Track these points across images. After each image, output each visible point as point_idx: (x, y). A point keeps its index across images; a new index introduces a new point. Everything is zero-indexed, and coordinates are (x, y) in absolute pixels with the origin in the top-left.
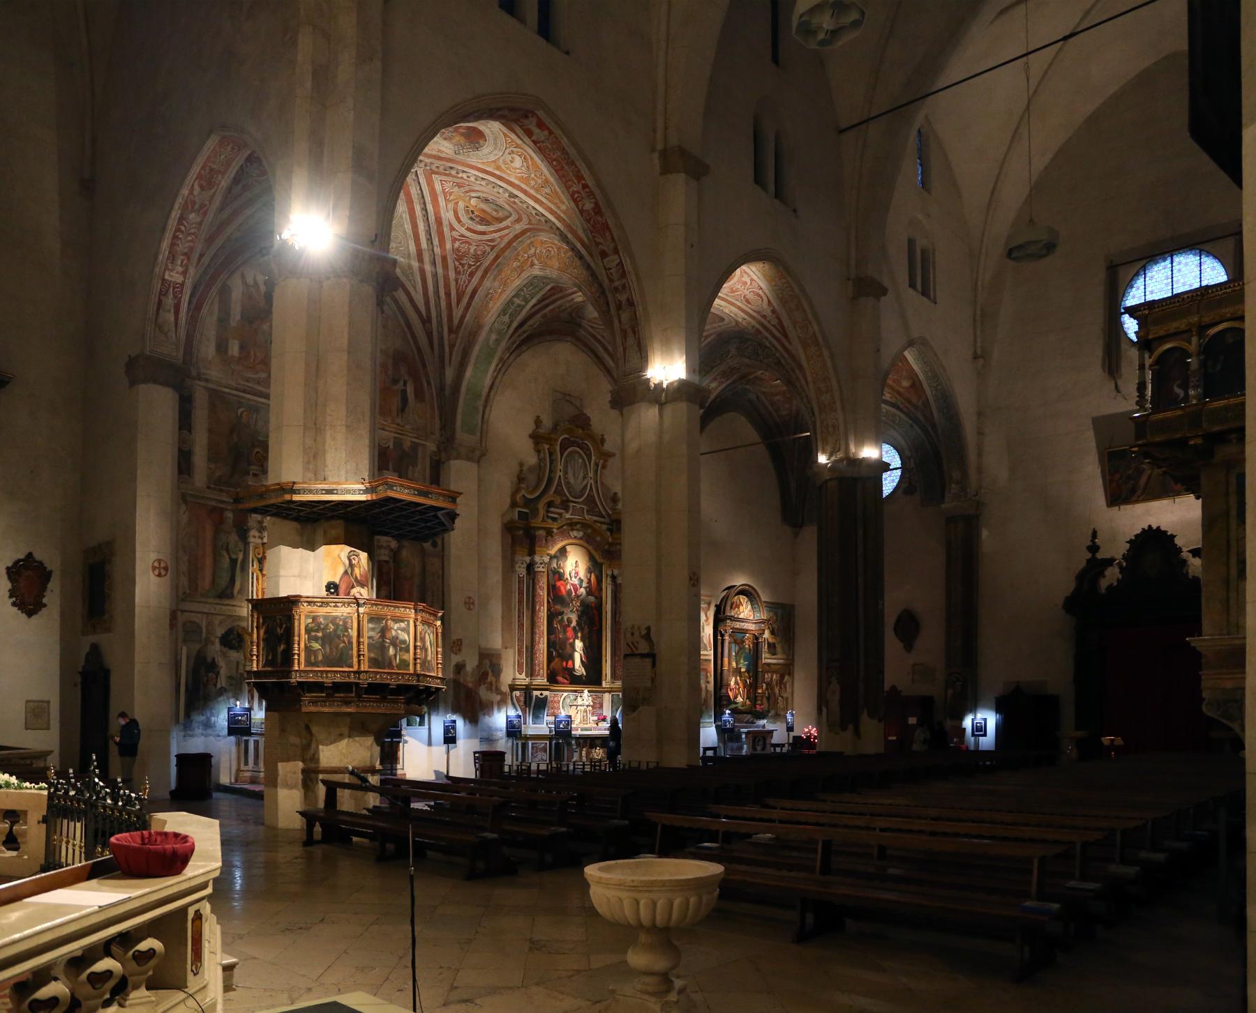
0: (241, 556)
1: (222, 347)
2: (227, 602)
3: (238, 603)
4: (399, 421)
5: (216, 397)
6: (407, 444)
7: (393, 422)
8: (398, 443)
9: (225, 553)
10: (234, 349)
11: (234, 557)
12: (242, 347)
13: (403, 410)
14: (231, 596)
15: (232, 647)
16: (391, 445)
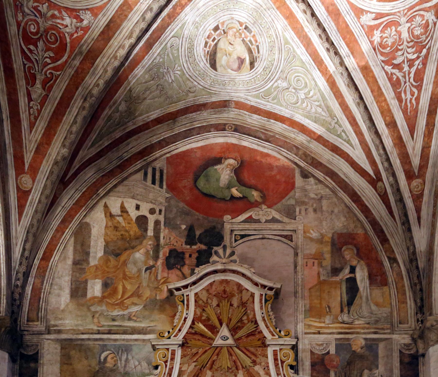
1: (78, 291)
4: (345, 318)
5: (70, 348)
6: (358, 343)
7: (335, 320)
8: (342, 346)
10: (95, 288)
12: (105, 285)
13: (350, 303)
16: (333, 351)
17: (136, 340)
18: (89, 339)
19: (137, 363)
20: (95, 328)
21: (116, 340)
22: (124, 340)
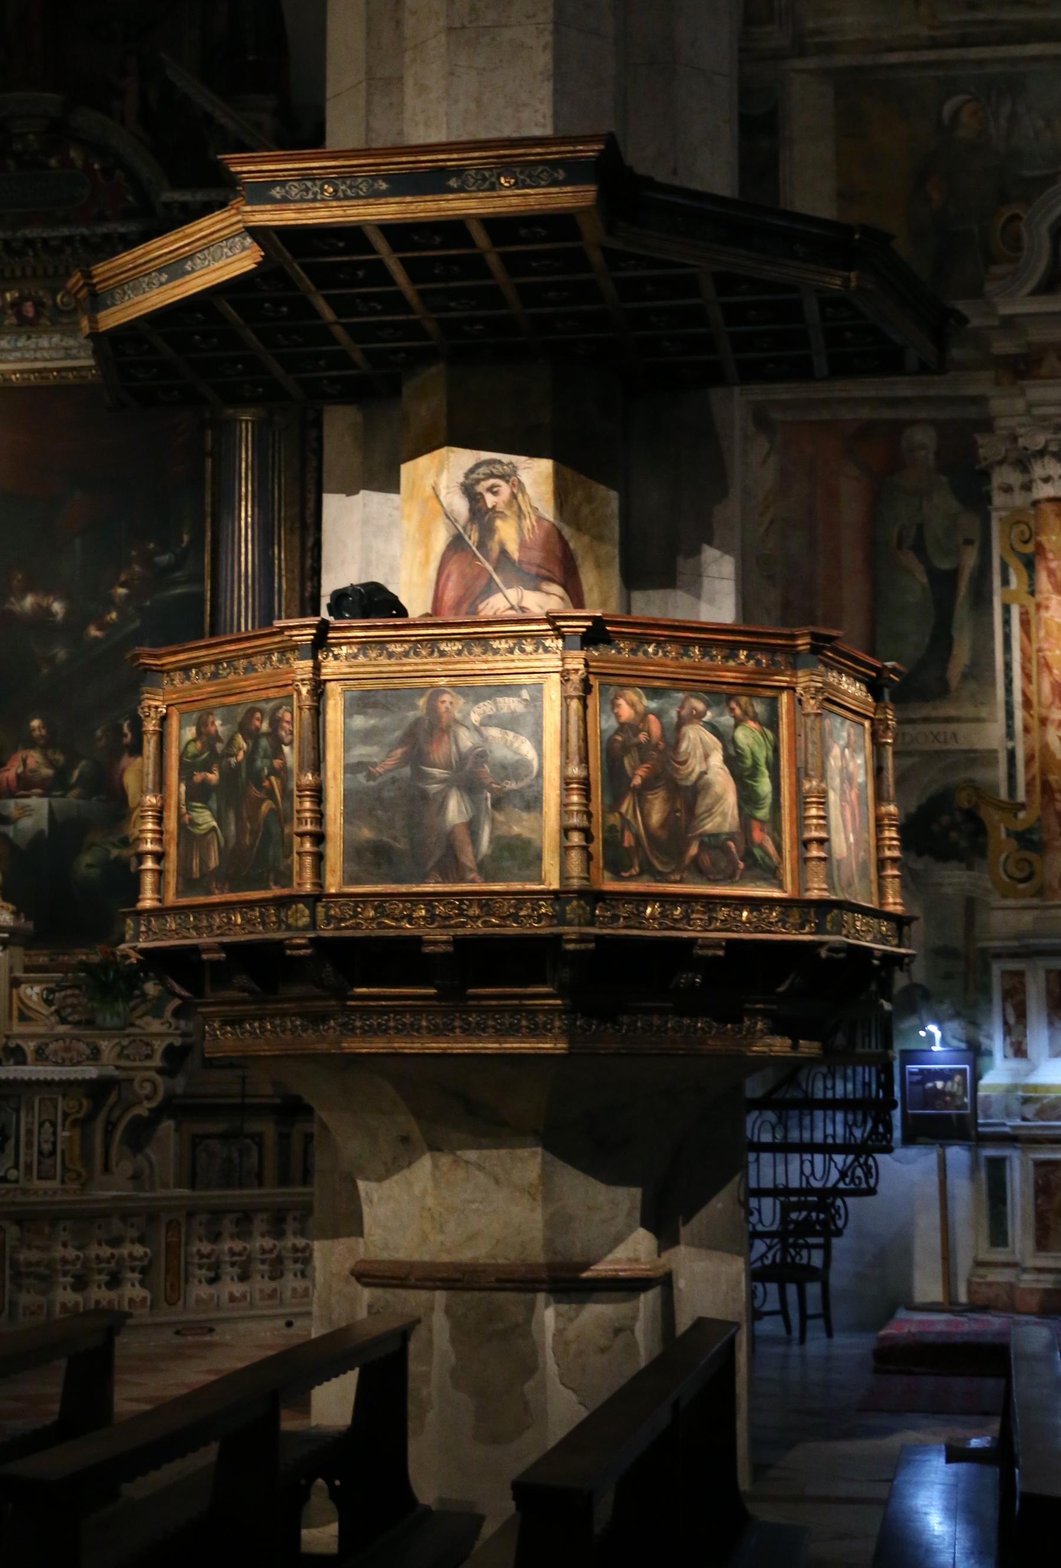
0: (970, 559)
2: (927, 711)
3: (969, 710)
9: (910, 560)
11: (944, 565)
14: (942, 691)
15: (946, 853)
17: (1036, 59)
18: (907, 65)
19: (1041, 124)
20: (925, 32)
21: (980, 63)
22: (1001, 61)
